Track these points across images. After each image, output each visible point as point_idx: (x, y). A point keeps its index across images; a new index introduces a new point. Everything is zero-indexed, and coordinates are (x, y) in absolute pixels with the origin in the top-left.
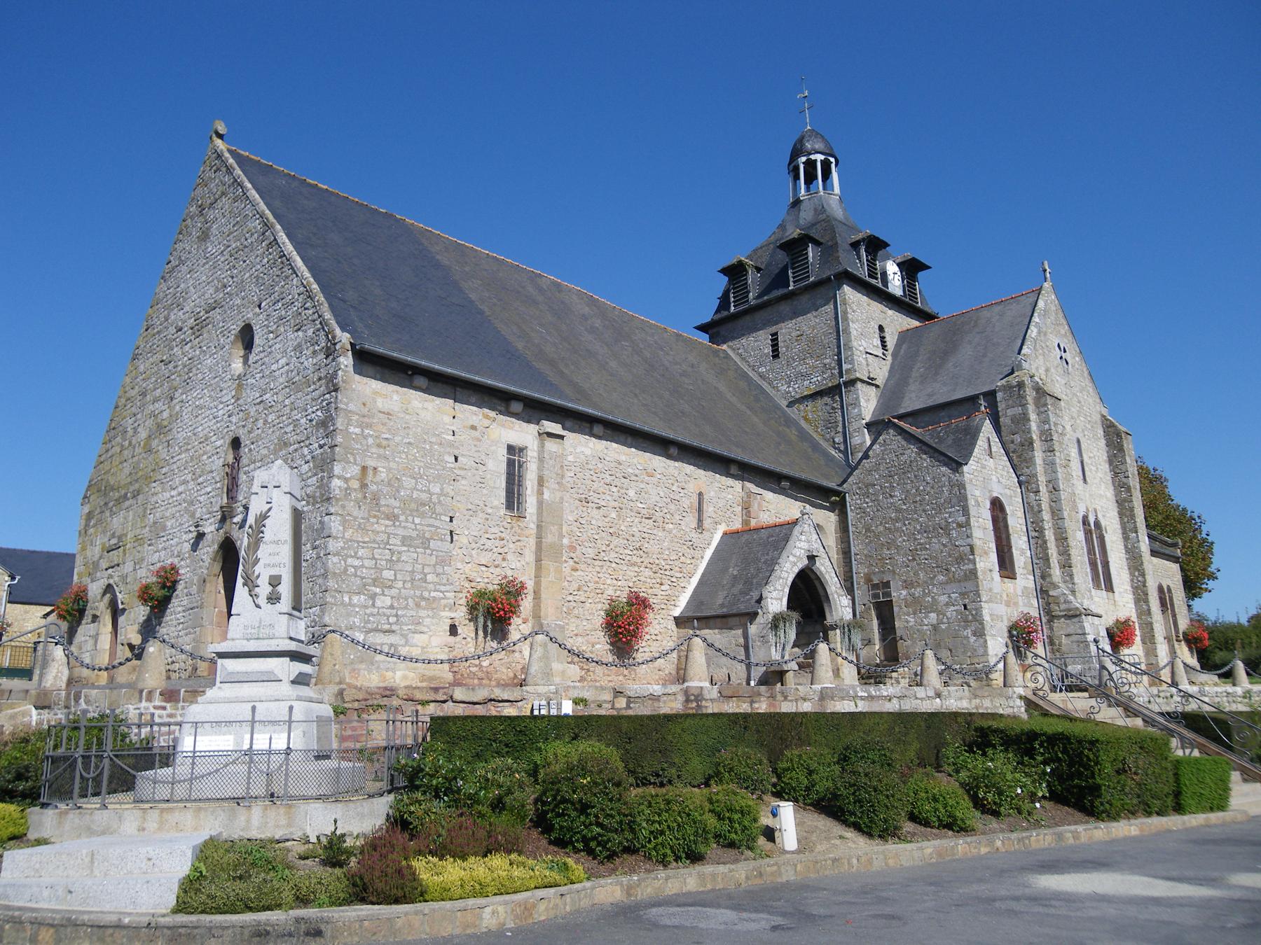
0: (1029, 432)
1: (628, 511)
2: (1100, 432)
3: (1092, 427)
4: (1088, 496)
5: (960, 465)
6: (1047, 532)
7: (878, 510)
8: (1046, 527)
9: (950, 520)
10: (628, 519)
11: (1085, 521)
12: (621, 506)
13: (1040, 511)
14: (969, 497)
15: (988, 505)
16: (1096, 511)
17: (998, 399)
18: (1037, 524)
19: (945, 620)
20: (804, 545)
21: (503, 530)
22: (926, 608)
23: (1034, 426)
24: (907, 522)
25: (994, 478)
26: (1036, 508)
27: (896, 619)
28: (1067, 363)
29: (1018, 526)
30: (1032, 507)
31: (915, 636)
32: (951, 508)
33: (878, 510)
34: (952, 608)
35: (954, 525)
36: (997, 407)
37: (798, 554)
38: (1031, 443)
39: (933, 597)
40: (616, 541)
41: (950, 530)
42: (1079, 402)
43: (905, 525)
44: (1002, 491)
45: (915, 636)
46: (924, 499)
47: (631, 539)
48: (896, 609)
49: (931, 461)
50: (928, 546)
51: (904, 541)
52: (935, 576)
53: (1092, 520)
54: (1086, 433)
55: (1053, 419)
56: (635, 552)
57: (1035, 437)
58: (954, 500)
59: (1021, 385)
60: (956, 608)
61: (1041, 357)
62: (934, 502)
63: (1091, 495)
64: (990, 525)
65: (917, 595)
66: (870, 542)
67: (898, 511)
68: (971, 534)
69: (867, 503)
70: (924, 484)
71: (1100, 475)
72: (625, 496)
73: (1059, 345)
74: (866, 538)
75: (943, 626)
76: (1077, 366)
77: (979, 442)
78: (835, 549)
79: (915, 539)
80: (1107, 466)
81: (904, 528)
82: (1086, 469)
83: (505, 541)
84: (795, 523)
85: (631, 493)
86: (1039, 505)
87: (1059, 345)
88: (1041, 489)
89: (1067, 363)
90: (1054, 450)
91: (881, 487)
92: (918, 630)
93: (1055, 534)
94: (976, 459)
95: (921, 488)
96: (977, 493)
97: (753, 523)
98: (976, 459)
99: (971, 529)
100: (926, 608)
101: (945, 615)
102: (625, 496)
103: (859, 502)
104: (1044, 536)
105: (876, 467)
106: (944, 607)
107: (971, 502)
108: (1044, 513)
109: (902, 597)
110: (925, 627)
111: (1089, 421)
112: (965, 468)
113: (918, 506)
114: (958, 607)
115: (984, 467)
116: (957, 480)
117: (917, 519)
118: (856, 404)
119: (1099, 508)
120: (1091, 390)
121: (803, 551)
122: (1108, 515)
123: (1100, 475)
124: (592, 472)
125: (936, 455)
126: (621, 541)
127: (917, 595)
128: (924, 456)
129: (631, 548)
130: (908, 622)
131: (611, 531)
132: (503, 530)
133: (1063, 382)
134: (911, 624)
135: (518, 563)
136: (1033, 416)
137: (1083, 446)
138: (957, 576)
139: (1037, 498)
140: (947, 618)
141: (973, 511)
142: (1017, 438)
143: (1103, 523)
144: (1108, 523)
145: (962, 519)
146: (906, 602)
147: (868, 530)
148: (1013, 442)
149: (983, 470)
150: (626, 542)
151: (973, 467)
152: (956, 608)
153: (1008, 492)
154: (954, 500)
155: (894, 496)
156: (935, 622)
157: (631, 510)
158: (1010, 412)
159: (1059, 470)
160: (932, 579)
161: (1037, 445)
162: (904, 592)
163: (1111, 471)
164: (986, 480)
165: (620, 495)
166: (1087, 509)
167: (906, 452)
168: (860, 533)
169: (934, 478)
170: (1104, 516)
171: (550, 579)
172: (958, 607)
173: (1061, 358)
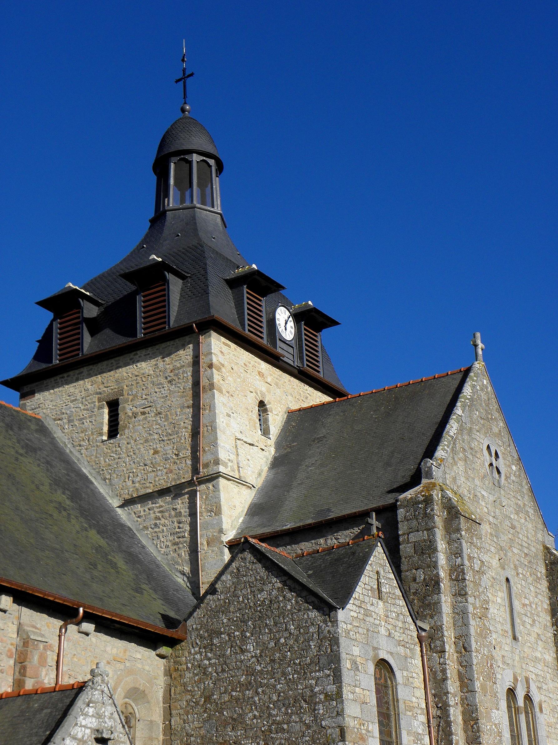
0: (435, 565)
2: (542, 570)
3: (530, 562)
4: (517, 658)
5: (333, 609)
6: (452, 710)
7: (223, 671)
8: (451, 703)
9: (317, 689)
11: (511, 692)
13: (445, 679)
14: (343, 656)
15: (371, 668)
16: (527, 680)
17: (400, 518)
18: (440, 698)
20: (92, 723)
23: (442, 559)
24: (260, 690)
25: (383, 631)
26: (440, 676)
28: (499, 472)
29: (414, 699)
30: (435, 673)
32: (319, 671)
33: (223, 671)
35: (322, 697)
36: (397, 529)
37: (80, 736)
38: (436, 582)
41: (315, 704)
42: (513, 527)
43: (258, 694)
44: (394, 650)
46: (285, 657)
49: (297, 602)
50: (285, 726)
53: (520, 694)
54: (520, 570)
55: (466, 550)
57: (442, 574)
58: (323, 660)
59: (428, 500)
61: (461, 464)
62: (297, 661)
63: (522, 658)
64: (372, 699)
66: (210, 717)
67: (251, 672)
68: (343, 709)
69: (209, 659)
70: (286, 634)
71: (537, 629)
73: (488, 447)
74: (205, 712)
76: (513, 478)
77: (364, 579)
79: (270, 715)
80: (549, 618)
81: (256, 699)
82: (517, 621)
84: (81, 688)
86: (444, 671)
87: (488, 447)
88: (447, 647)
89: (499, 472)
90: (466, 594)
91: (229, 635)
93: (463, 713)
94: (357, 602)
95: (282, 640)
96: (356, 651)
97: (29, 685)
98: (357, 602)
99: (342, 702)
103: (198, 657)
104: (448, 716)
105: (224, 609)
107: (346, 665)
108: (449, 682)
111: (526, 555)
112: (341, 614)
113: (277, 666)
115: (368, 613)
116: (329, 631)
117: (274, 686)
118: (216, 510)
119: (532, 676)
120: (531, 511)
121: (88, 731)
122: (545, 687)
123: (537, 629)
125: (304, 593)
128: (289, 595)
133: (492, 498)
136: (441, 545)
137: (514, 589)
139: (442, 660)
141: (347, 677)
142: (421, 575)
143: (536, 698)
144: (543, 698)
145: (331, 688)
147: (208, 699)
148: (415, 580)
149: (368, 619)
151: (352, 614)
153: (401, 650)
154: (323, 660)
155: (248, 651)
158: (413, 537)
159: (472, 622)
161: (445, 585)
163: (553, 625)
164: (371, 632)
166: (516, 679)
167: (265, 588)
168: (197, 703)
169: (298, 628)
170: (539, 688)
173: (491, 465)
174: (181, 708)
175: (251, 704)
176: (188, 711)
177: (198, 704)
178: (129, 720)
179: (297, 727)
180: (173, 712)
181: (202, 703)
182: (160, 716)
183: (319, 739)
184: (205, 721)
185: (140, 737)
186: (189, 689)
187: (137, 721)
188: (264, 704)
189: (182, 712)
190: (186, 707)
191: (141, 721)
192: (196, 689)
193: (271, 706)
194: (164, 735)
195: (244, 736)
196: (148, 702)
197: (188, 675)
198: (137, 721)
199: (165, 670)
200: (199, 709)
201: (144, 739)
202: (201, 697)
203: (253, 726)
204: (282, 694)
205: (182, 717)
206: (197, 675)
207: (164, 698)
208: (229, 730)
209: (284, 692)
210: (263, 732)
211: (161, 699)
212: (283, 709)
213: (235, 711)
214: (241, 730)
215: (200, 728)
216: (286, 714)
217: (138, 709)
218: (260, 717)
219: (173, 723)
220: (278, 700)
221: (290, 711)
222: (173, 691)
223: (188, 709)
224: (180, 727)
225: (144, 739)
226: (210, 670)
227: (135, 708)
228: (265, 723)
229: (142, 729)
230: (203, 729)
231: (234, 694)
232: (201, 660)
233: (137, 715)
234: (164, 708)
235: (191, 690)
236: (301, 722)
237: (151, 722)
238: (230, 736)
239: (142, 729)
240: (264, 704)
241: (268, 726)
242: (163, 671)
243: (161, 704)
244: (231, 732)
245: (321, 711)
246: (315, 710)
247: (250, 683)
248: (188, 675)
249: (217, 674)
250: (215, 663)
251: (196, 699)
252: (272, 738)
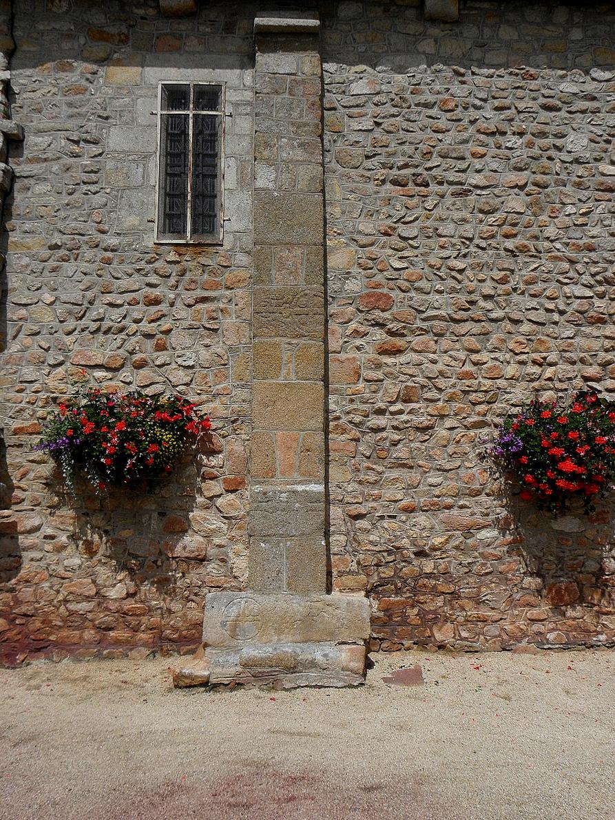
1: (569, 189)
10: (570, 209)
12: (539, 178)
21: (153, 279)
40: (525, 269)
47: (585, 257)
56: (601, 289)
72: (552, 153)
83: (164, 307)
85: (577, 143)
102: (552, 153)
124: (434, 112)
126: (550, 266)
129: (586, 279)
131: (510, 244)
132: (153, 279)
135: (203, 351)
150: (566, 266)
157: (578, 185)
165: (536, 151)
171: (281, 381)
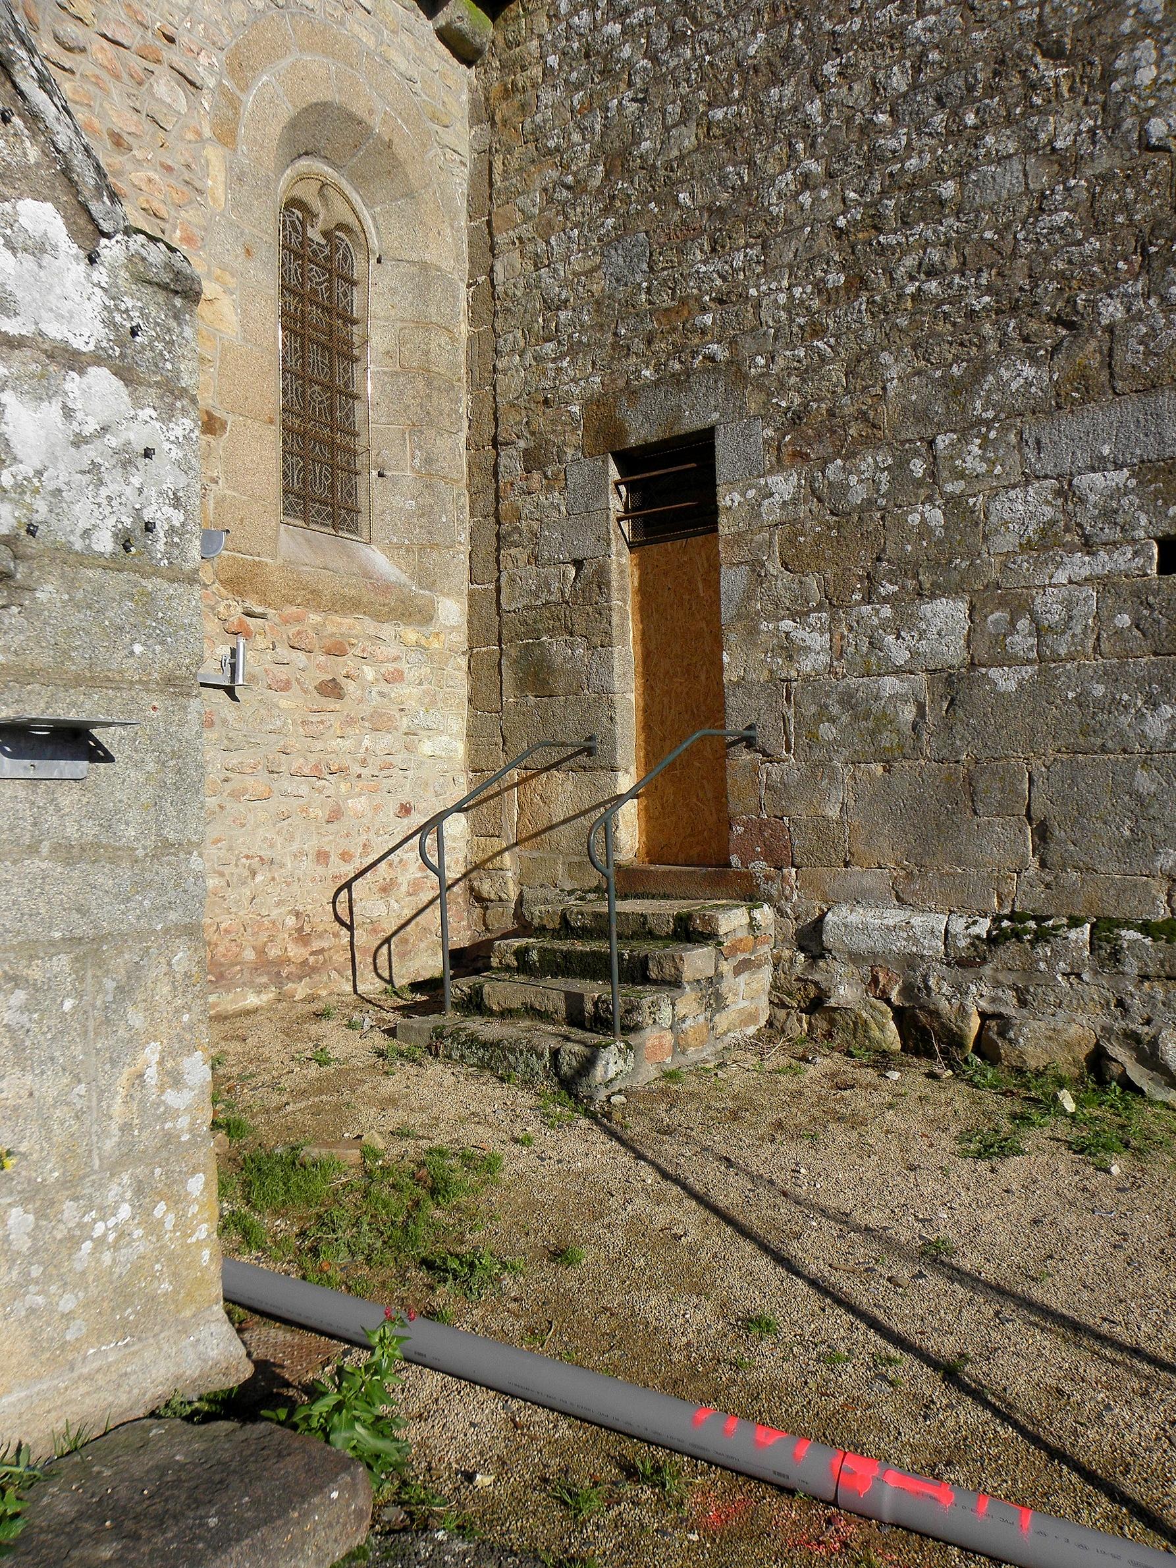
7: (677, 39)
19: (1022, 641)
22: (906, 568)
24: (830, 69)
27: (732, 638)
31: (827, 731)
33: (677, 39)
34: (1079, 565)
39: (954, 504)
43: (818, 85)
45: (827, 731)
48: (732, 581)
50: (948, 189)
51: (806, 182)
52: (981, 369)
60: (1104, 563)
65: (858, 493)
66: (624, 228)
74: (606, 211)
75: (1005, 680)
78: (463, 293)
79: (875, 157)
81: (814, 109)
92: (847, 700)
100: (906, 568)
101: (1018, 605)
106: (1024, 563)
109: (771, 511)
110: (890, 685)
114: (1123, 559)
117: (897, 33)
127: (858, 493)
130: (789, 650)
134: (807, 664)
138: (1131, 354)
140: (1039, 631)
146: (791, 540)
152: (1104, 563)
156: (954, 652)
160: (959, 390)
162: (784, 485)
168: (579, 188)
172: (1123, 559)
174: (527, 218)
175: (789, 137)
176: (550, 224)
177: (584, 191)
178: (345, 258)
179: (1009, 179)
180: (500, 239)
181: (596, 182)
182: (457, 258)
183: (1126, 207)
184: (607, 243)
185: (387, 319)
186: (551, 144)
187: (373, 261)
188: (849, 120)
189: (527, 230)
190: (542, 211)
191: (388, 264)
192: (576, 137)
193: (882, 118)
194: (472, 322)
195: (759, 269)
196: (410, 195)
197: (548, 96)
198: (373, 261)
199: (474, 102)
200: (589, 206)
201: (399, 325)
202: (593, 160)
203: (797, 222)
204: (934, 56)
205: (530, 247)
206: (579, 86)
207: (471, 200)
208: (699, 256)
209: (939, 47)
210: (840, 233)
211: (461, 204)
212: (937, 119)
213: (723, 179)
214: (747, 246)
215: (589, 273)
216: (954, 133)
217: (374, 218)
218: (831, 175)
219: (499, 276)
220: (914, 87)
221: (971, 119)
222: (498, 167)
223: (549, 214)
224: (521, 282)
225: (399, 325)
226: (626, 52)
227: (365, 214)
228: (853, 195)
229: (393, 291)
230: (600, 273)
231: (719, 114)
232: (595, 27)
233: (374, 242)
234: (472, 231)
235: (557, 149)
236: (1029, 151)
237: (424, 266)
238: (701, 279)
239: (393, 291)
240: (849, 120)
241: (867, 205)
242: (467, 106)
243: (463, 221)
244: (705, 262)
245: (1146, 75)
246: (1109, 76)
247: (786, 54)
248: (548, 96)
249: (654, 59)
250: (646, 23)
251: (575, 174)
252: (882, 250)
